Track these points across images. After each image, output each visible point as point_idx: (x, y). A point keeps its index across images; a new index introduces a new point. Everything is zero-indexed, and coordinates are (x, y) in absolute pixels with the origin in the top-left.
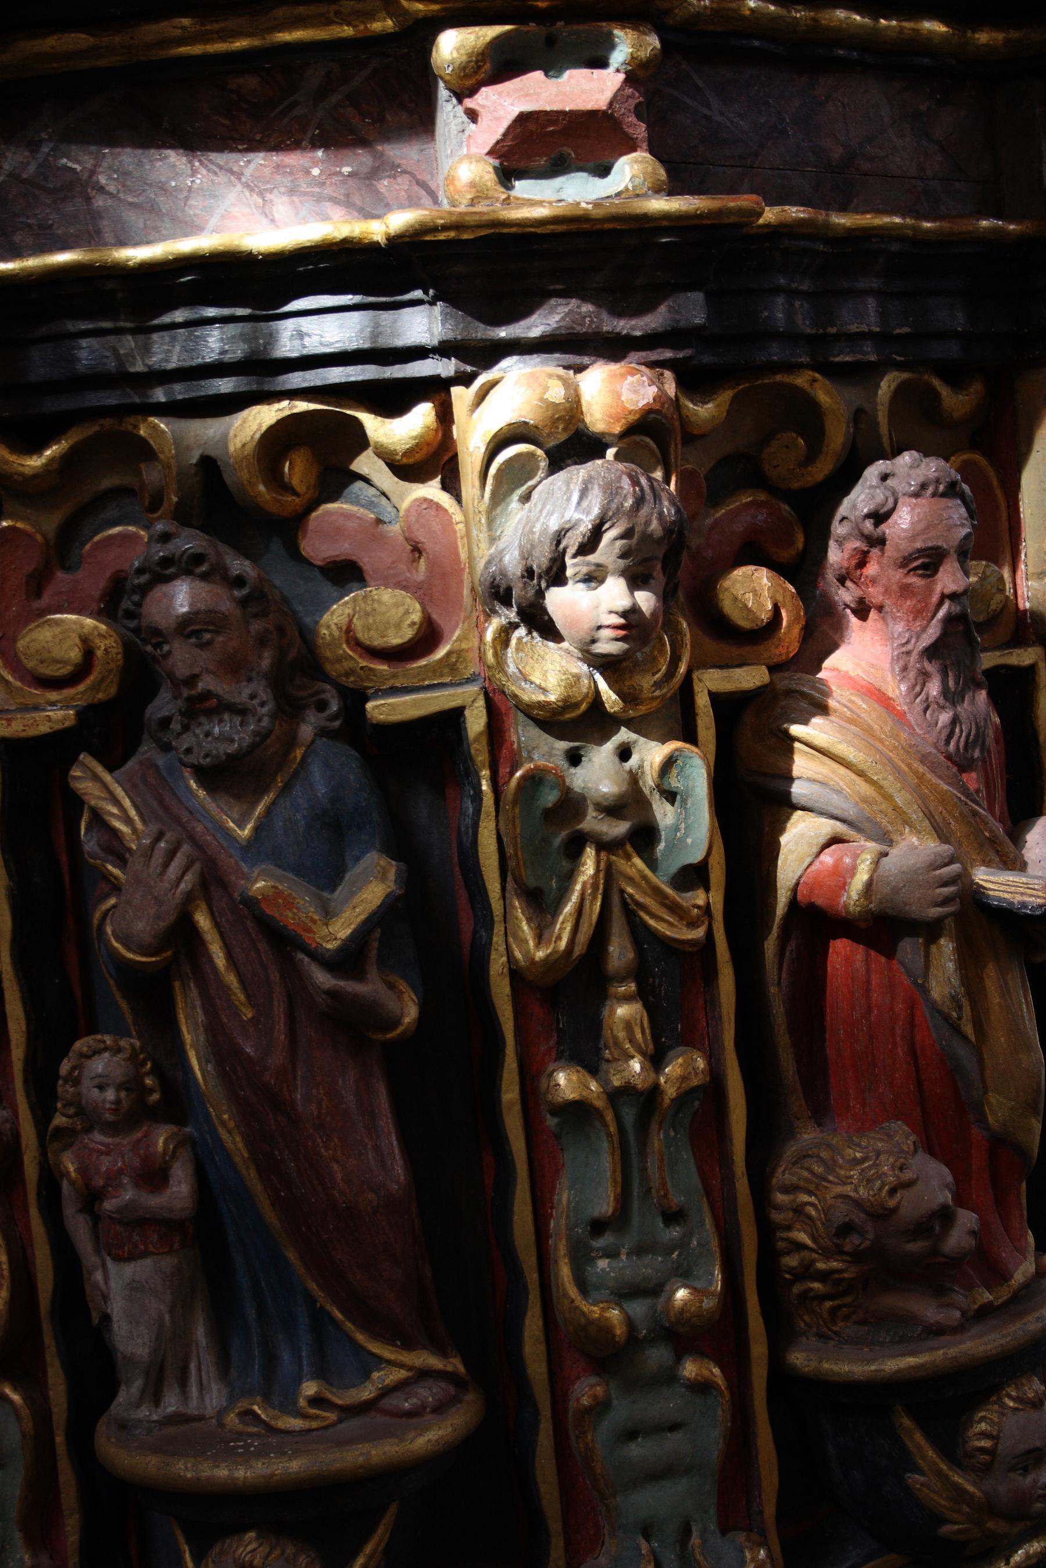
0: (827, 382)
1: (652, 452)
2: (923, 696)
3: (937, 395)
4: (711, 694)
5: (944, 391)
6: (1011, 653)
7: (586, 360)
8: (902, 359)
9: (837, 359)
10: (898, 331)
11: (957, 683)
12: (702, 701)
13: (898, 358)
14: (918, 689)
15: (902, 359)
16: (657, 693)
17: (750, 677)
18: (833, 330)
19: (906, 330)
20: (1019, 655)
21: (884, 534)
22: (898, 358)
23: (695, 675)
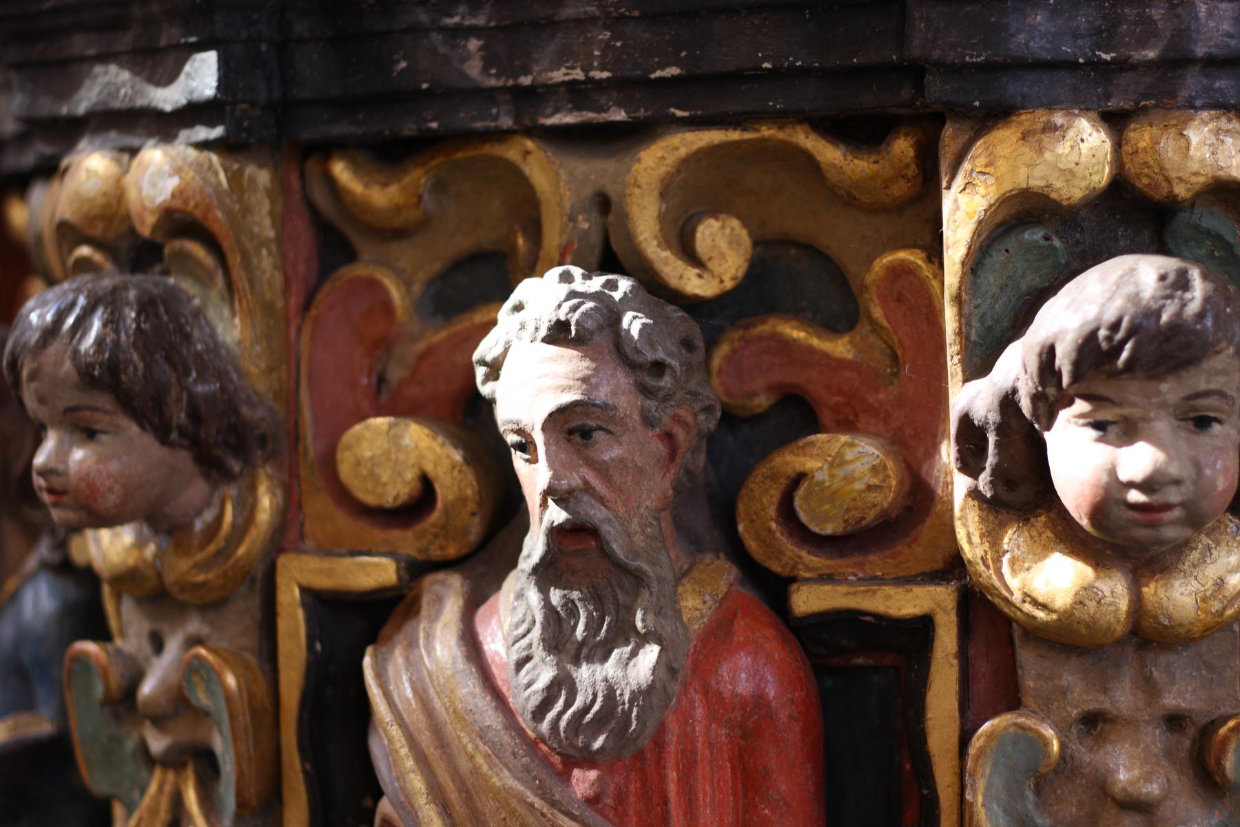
0: (542, 154)
1: (199, 263)
2: (524, 642)
3: (808, 161)
4: (305, 590)
5: (829, 154)
6: (874, 592)
7: (134, 141)
8: (686, 114)
9: (549, 121)
10: (658, 74)
11: (593, 627)
12: (289, 597)
13: (679, 113)
14: (521, 630)
15: (686, 114)
16: (201, 578)
17: (376, 571)
18: (526, 81)
19: (674, 71)
20: (888, 597)
21: (494, 392)
22: (679, 113)
23: (283, 561)
